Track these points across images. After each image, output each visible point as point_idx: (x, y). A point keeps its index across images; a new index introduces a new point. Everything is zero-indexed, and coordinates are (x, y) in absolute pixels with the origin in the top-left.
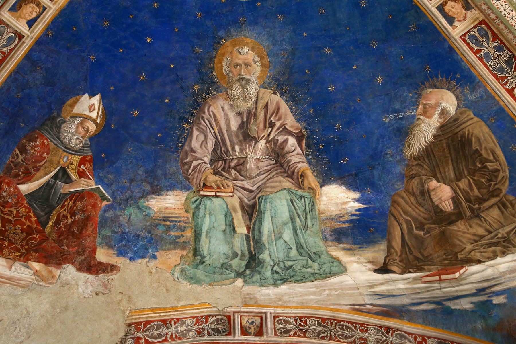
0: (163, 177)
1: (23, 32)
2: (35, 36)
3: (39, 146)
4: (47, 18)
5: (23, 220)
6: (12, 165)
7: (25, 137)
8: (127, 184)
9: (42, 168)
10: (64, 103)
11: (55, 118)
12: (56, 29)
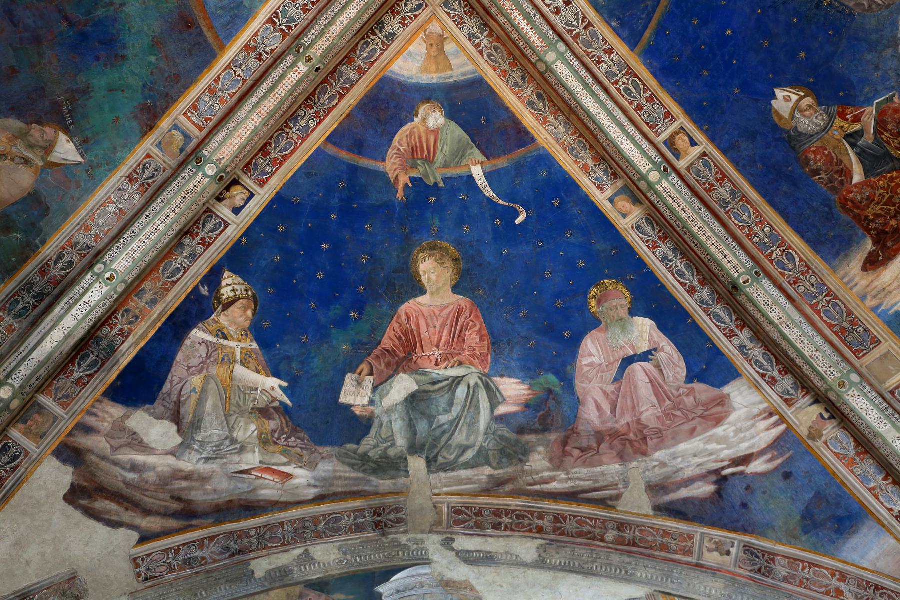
0: (880, 33)
3: (816, 157)
5: (893, 185)
6: (829, 185)
7: (803, 168)
8: (880, 73)
9: (840, 157)
10: (776, 125)
11: (790, 137)
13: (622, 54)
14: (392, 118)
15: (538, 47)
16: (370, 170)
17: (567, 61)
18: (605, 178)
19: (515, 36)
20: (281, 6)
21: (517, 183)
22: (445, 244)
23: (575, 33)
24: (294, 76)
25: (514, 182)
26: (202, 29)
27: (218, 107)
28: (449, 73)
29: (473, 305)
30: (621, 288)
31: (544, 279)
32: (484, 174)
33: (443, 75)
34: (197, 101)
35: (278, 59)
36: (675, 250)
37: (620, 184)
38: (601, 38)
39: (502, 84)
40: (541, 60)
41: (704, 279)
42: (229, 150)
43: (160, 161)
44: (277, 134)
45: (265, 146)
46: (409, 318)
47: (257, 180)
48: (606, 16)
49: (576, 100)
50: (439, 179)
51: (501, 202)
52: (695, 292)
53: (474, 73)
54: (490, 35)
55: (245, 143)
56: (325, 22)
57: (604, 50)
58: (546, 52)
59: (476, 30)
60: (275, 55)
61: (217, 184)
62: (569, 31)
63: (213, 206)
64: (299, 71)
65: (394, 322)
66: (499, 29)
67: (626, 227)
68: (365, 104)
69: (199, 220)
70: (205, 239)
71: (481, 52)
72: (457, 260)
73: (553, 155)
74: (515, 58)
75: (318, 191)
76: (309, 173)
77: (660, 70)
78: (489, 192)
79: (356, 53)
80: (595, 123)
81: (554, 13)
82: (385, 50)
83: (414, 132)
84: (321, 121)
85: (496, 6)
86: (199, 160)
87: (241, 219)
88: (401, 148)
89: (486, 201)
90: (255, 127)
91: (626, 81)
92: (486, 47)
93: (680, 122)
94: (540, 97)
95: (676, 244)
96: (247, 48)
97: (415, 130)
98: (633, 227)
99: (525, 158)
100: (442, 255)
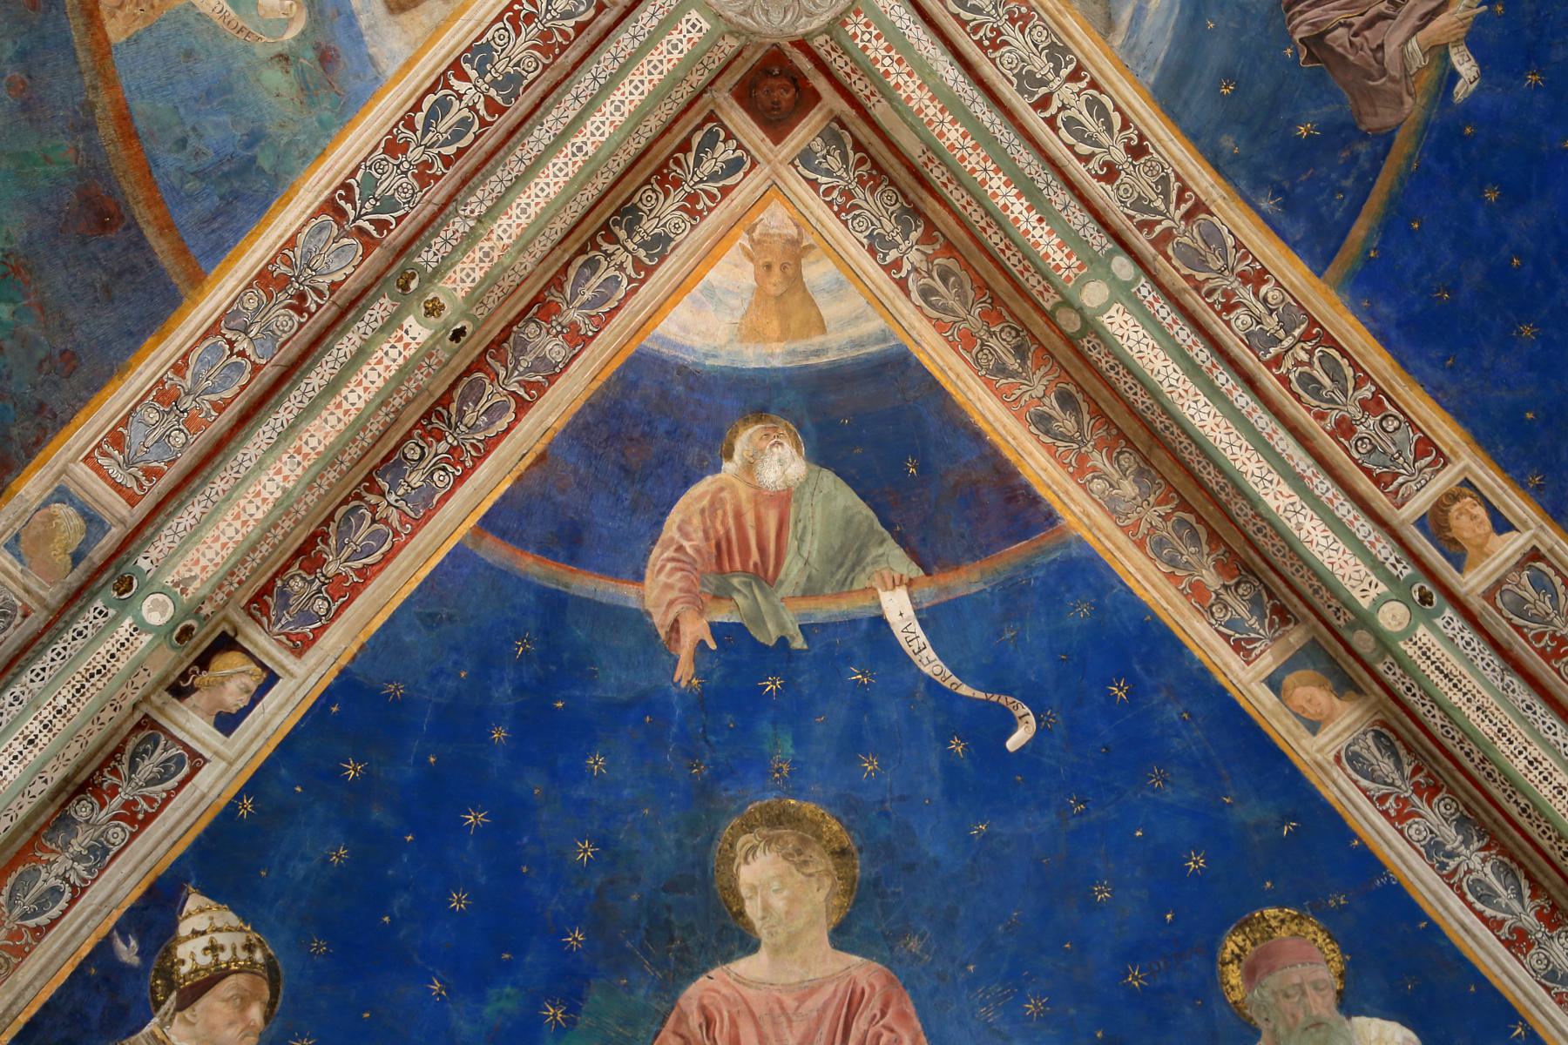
1: (1522, 547)
2: (1538, 519)
4: (1494, 480)
12: (1525, 463)
13: (1292, 284)
14: (661, 464)
15: (1058, 267)
16: (601, 604)
17: (1139, 303)
18: (1253, 622)
19: (996, 239)
20: (358, 167)
21: (1008, 635)
22: (809, 808)
23: (1158, 229)
24: (393, 353)
25: (999, 634)
26: (140, 231)
27: (181, 439)
28: (817, 340)
29: (890, 981)
30: (1311, 929)
31: (1090, 905)
32: (917, 612)
33: (800, 345)
34: (124, 422)
35: (351, 307)
36: (1462, 823)
37: (1296, 637)
38: (1230, 241)
39: (961, 367)
40: (1067, 303)
41: (1554, 907)
42: (210, 554)
43: (13, 586)
44: (344, 509)
45: (311, 541)
46: (709, 1023)
47: (288, 636)
48: (1243, 184)
49: (1166, 411)
50: (793, 630)
51: (965, 690)
52: (1530, 946)
53: (885, 340)
54: (927, 238)
55: (254, 536)
56: (480, 210)
57: (1242, 275)
58: (1081, 282)
59: (888, 226)
60: (342, 297)
61: (174, 648)
62: (1141, 225)
63: (161, 710)
64: (407, 339)
65: (666, 1033)
66: (952, 221)
67: (1319, 757)
68: (586, 427)
69: (120, 749)
70: (135, 803)
71: (902, 284)
72: (843, 852)
73: (1107, 557)
74: (995, 299)
75: (455, 663)
76: (432, 616)
77: (1399, 325)
78: (930, 663)
79: (562, 291)
80: (1220, 470)
81: (1099, 178)
82: (643, 282)
83: (722, 500)
84: (467, 473)
85: (943, 162)
86: (124, 585)
87: (239, 745)
88: (686, 544)
89: (922, 686)
90: (284, 490)
91: (1304, 356)
92: (916, 269)
93: (1460, 466)
94: (1066, 400)
95: (1467, 807)
96: (264, 279)
97: (725, 494)
98: (1338, 759)
99: (1028, 568)
100: (803, 840)
